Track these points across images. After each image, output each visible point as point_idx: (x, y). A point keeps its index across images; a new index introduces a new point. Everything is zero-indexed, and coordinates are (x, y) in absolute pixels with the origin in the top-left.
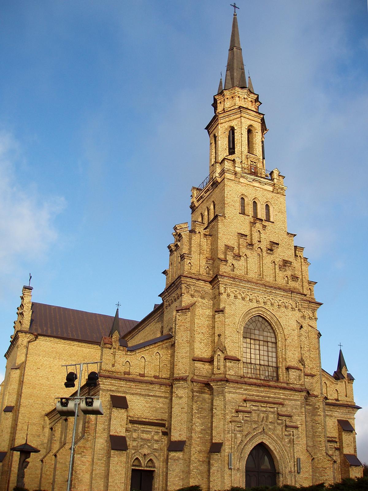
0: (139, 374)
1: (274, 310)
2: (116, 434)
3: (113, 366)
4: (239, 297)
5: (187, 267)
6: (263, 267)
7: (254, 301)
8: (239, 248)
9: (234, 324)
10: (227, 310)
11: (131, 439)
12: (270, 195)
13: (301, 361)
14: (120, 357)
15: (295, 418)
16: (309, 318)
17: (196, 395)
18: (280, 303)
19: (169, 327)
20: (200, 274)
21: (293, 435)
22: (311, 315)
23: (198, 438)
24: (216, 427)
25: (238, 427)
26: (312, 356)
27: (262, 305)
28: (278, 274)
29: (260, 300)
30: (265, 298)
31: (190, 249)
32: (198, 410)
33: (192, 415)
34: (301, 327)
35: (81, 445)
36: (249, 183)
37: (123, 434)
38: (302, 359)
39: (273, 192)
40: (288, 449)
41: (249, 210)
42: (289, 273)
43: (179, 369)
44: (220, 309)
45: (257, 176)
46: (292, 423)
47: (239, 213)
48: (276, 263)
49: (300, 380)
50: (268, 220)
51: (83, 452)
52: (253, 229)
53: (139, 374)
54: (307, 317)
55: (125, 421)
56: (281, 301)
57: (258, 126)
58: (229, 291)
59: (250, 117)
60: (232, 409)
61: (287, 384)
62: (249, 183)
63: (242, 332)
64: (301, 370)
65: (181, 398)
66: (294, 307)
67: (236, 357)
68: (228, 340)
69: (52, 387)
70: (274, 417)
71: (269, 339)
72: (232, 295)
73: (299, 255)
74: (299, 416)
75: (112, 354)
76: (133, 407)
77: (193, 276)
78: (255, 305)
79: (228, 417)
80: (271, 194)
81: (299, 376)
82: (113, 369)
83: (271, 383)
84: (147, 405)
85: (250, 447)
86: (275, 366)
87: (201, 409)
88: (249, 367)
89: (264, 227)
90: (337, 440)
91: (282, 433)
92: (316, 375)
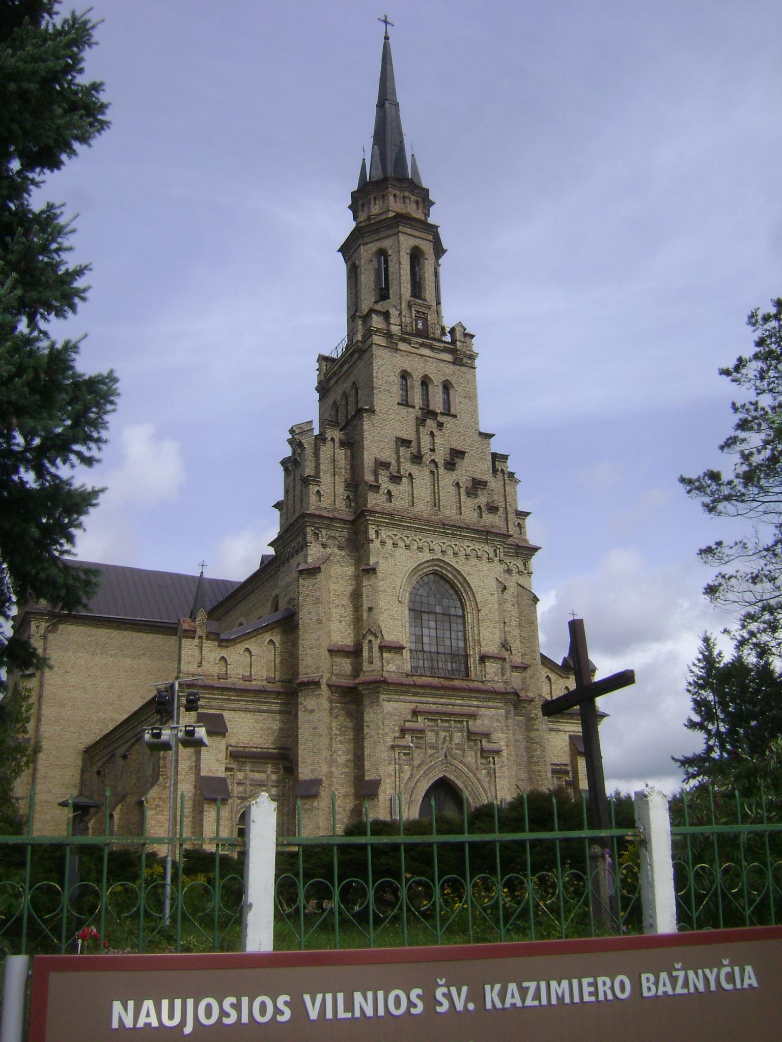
0: (243, 676)
1: (459, 564)
2: (211, 774)
3: (200, 665)
4: (401, 544)
5: (313, 499)
6: (439, 493)
7: (426, 550)
8: (398, 462)
9: (394, 588)
10: (382, 568)
11: (235, 781)
13: (505, 646)
14: (210, 651)
15: (496, 736)
16: (519, 572)
17: (336, 707)
18: (468, 552)
19: (288, 597)
20: (336, 509)
21: (494, 763)
22: (522, 568)
23: (341, 774)
24: (370, 756)
25: (405, 754)
26: (524, 635)
27: (439, 556)
28: (464, 502)
29: (435, 547)
30: (444, 543)
31: (317, 468)
32: (339, 730)
33: (331, 739)
34: (505, 588)
35: (155, 795)
36: (413, 350)
37: (221, 773)
38: (506, 640)
39: (454, 363)
40: (486, 785)
41: (417, 398)
42: (482, 500)
43: (307, 666)
44: (369, 565)
45: (427, 338)
46: (492, 744)
47: (399, 404)
48: (461, 485)
49: (503, 674)
50: (447, 413)
51: (158, 806)
52: (421, 429)
53: (243, 676)
54: (516, 570)
55: (224, 754)
56: (470, 548)
57: (427, 248)
60: (394, 725)
61: (483, 682)
62: (413, 350)
63: (407, 601)
64: (505, 659)
65: (312, 711)
66: (492, 555)
67: (398, 642)
68: (385, 615)
69: (93, 703)
70: (463, 736)
71: (453, 612)
72: (389, 542)
73: (500, 469)
74: (502, 733)
75: (196, 646)
76: (235, 731)
77: (326, 514)
78: (427, 556)
79: (389, 741)
80: (451, 367)
81: (503, 669)
82: (200, 670)
83: (457, 683)
84: (258, 726)
85: (425, 786)
86: (464, 654)
87: (345, 727)
88: (421, 657)
89: (440, 425)
90: (569, 768)
91: (476, 761)
92: (530, 666)
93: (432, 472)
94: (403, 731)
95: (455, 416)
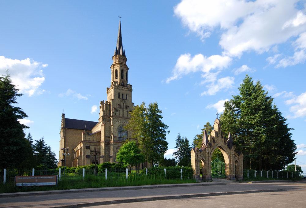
12: (127, 92)
41: (121, 97)
58: (114, 120)
59: (122, 66)
72: (115, 121)
78: (121, 123)
93: (123, 110)
94: (116, 149)
95: (128, 100)
